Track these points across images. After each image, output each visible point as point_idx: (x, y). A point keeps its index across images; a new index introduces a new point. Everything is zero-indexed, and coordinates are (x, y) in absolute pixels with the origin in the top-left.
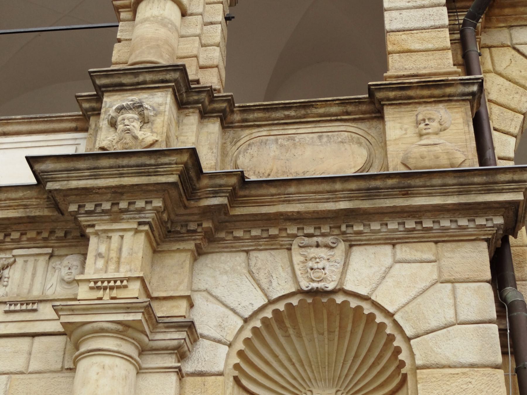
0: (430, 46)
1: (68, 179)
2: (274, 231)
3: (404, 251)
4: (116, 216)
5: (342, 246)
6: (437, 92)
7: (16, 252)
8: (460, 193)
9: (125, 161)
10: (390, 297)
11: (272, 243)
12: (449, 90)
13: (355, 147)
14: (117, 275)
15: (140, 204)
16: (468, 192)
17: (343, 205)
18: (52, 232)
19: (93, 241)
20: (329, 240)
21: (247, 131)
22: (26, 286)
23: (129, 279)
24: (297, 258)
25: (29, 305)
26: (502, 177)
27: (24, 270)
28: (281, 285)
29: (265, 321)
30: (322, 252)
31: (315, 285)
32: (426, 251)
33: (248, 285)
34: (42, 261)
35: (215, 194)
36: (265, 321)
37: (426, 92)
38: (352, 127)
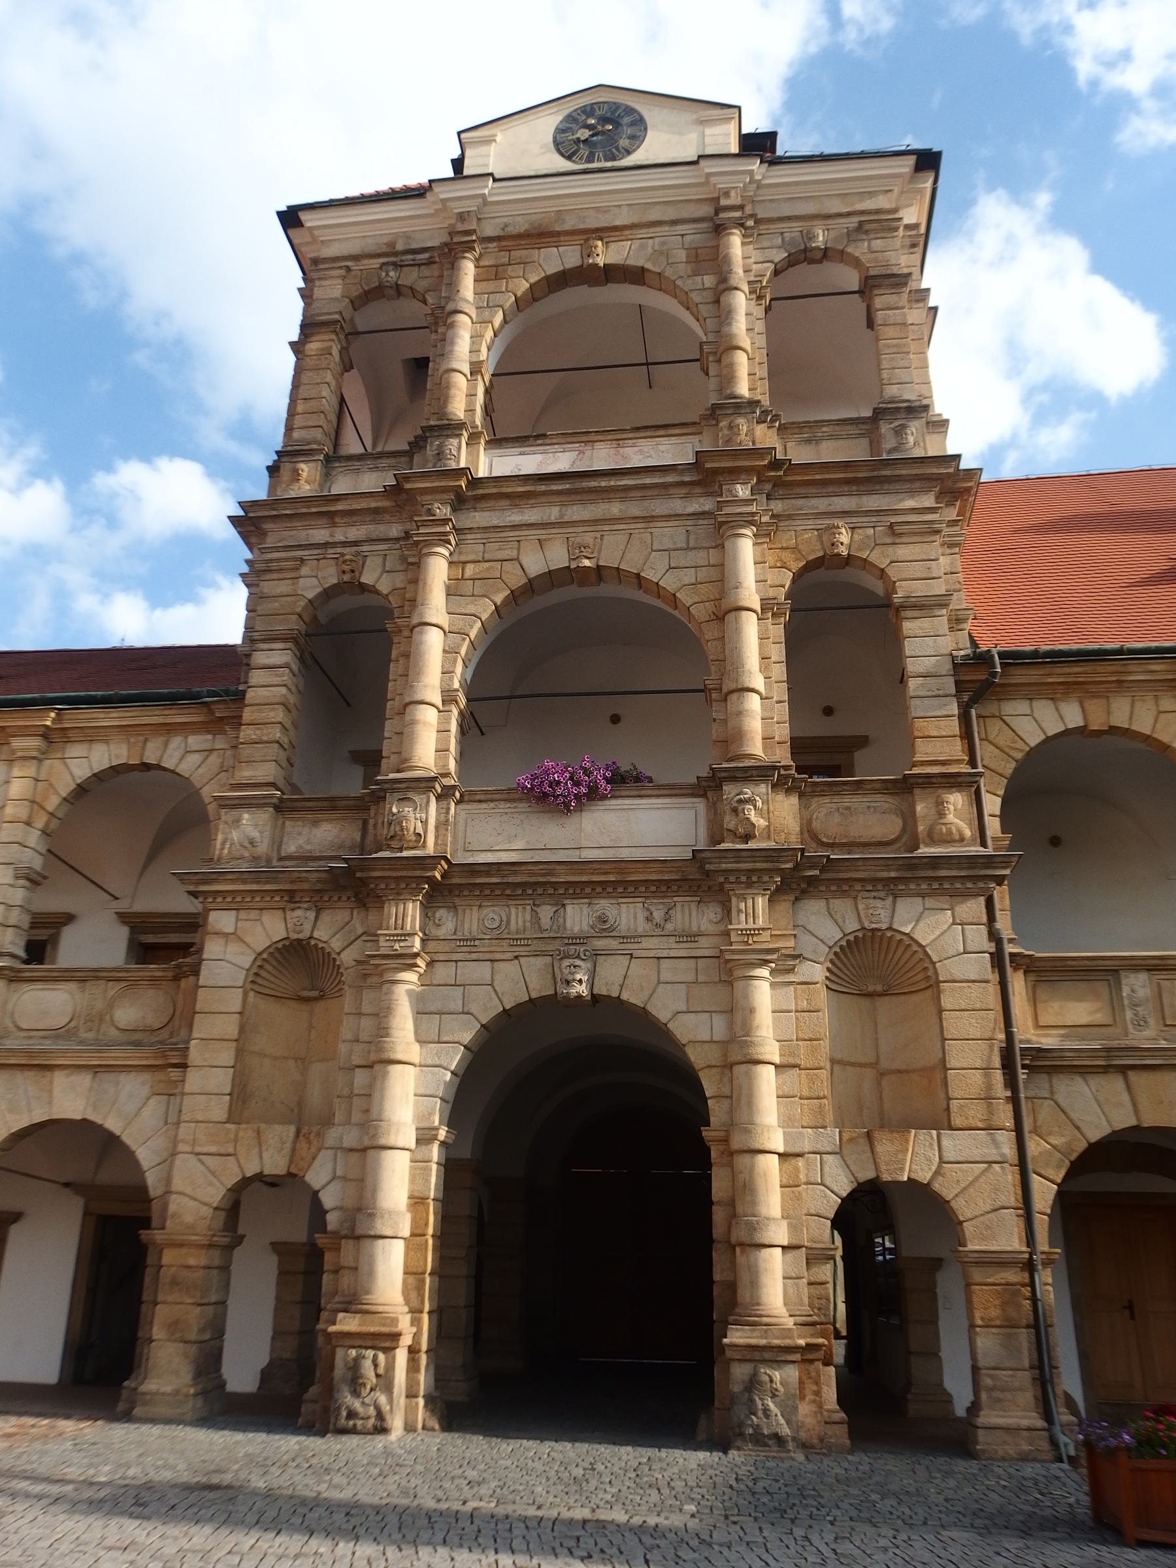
0: (944, 734)
1: (720, 863)
2: (845, 888)
3: (930, 902)
4: (749, 885)
5: (891, 898)
6: (952, 780)
7: (675, 899)
8: (969, 868)
9: (758, 854)
10: (924, 935)
11: (844, 894)
12: (960, 779)
13: (893, 816)
14: (755, 926)
15: (766, 878)
16: (974, 868)
17: (893, 874)
18: (699, 887)
19: (734, 900)
20: (882, 894)
21: (816, 799)
22: (687, 924)
23: (763, 929)
24: (861, 907)
25: (693, 937)
26: (996, 860)
27: (683, 911)
28: (852, 925)
29: (841, 947)
30: (879, 903)
31: (874, 926)
32: (943, 902)
33: (829, 923)
34: (693, 906)
35: (811, 868)
36: (841, 947)
37: (943, 780)
38: (889, 799)
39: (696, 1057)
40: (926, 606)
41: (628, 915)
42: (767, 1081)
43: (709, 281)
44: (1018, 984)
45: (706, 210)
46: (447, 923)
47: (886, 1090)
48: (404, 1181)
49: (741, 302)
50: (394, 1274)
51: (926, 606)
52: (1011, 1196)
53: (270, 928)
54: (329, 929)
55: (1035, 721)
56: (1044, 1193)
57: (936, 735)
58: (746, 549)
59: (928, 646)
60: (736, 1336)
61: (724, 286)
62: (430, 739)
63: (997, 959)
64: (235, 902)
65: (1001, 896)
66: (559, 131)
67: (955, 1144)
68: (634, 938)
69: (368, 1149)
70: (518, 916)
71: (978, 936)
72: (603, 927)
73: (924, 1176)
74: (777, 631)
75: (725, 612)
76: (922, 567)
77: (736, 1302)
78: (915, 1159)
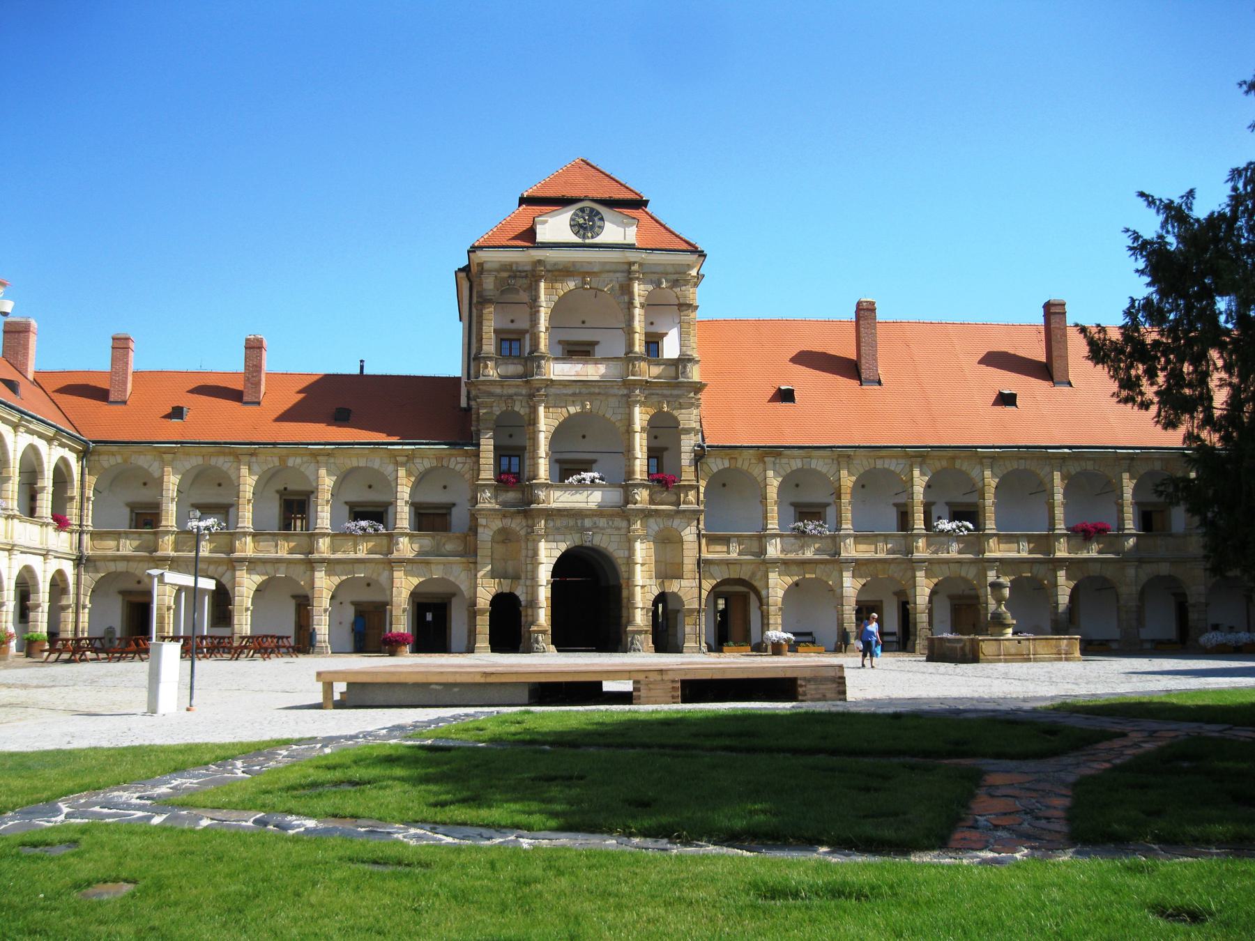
39: (619, 561)
40: (688, 431)
41: (602, 522)
42: (638, 568)
43: (626, 298)
44: (704, 541)
45: (626, 267)
46: (551, 524)
47: (667, 570)
48: (544, 594)
49: (638, 312)
50: (543, 617)
51: (688, 431)
52: (697, 595)
53: (497, 524)
54: (516, 524)
55: (716, 464)
56: (704, 594)
57: (688, 475)
58: (637, 410)
59: (688, 444)
60: (629, 628)
61: (630, 305)
62: (543, 469)
63: (698, 535)
64: (486, 517)
65: (702, 517)
66: (572, 219)
67: (684, 583)
68: (603, 529)
69: (534, 586)
70: (572, 522)
71: (694, 530)
72: (595, 526)
73: (676, 590)
74: (645, 435)
75: (629, 431)
76: (688, 418)
77: (630, 620)
78: (674, 587)
